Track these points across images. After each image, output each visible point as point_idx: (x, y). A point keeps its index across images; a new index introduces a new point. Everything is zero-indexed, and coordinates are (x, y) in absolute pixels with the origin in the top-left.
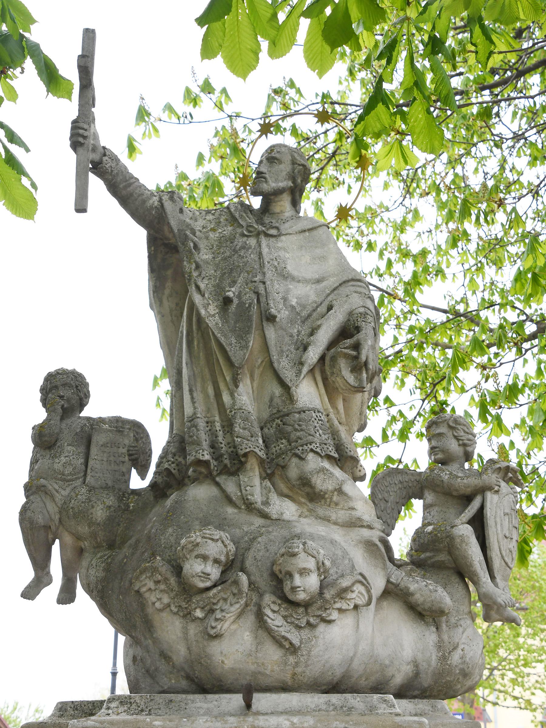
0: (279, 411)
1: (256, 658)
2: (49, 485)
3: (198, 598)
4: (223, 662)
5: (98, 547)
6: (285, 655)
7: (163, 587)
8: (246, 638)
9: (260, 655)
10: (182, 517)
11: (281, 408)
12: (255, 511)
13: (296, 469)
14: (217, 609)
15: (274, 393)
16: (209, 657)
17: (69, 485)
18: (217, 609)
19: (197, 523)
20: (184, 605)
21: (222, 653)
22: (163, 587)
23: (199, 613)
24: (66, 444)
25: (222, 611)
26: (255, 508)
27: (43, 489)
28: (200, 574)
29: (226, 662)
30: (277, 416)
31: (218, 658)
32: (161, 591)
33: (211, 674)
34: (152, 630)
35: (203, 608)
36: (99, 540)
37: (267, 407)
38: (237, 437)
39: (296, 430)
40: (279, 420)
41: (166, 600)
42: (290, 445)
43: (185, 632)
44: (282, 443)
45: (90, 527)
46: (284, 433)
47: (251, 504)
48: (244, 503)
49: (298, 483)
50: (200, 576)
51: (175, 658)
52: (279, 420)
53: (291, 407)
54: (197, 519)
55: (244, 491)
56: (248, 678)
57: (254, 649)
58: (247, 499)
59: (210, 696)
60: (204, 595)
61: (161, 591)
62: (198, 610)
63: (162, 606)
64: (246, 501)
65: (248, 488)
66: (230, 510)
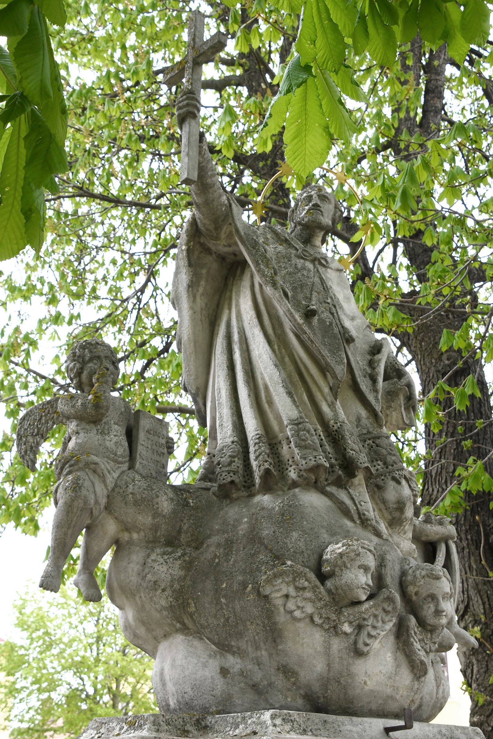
0: (369, 432)
1: (394, 681)
2: (101, 464)
3: (350, 610)
4: (365, 683)
5: (153, 542)
6: (413, 681)
7: (308, 594)
8: (388, 659)
9: (397, 678)
10: (305, 523)
11: (371, 430)
12: (370, 528)
13: (394, 492)
14: (368, 625)
15: (361, 414)
16: (351, 675)
17: (119, 467)
18: (368, 625)
19: (324, 531)
20: (333, 617)
21: (366, 673)
22: (308, 594)
23: (347, 628)
24: (112, 422)
25: (374, 627)
26: (371, 525)
27: (92, 466)
28: (364, 586)
29: (368, 683)
30: (368, 436)
31: (361, 678)
32: (305, 599)
33: (345, 694)
34: (278, 641)
35: (350, 623)
36: (159, 534)
37: (354, 426)
38: (352, 450)
39: (390, 454)
40: (371, 441)
41: (309, 609)
42: (387, 468)
43: (327, 647)
44: (379, 465)
45: (154, 517)
46: (379, 455)
47: (367, 520)
48: (360, 518)
49: (395, 506)
50: (364, 588)
51: (302, 674)
52: (371, 441)
53: (379, 430)
54: (322, 527)
55: (359, 506)
56: (380, 701)
57: (393, 672)
58: (364, 515)
59: (355, 719)
60: (356, 609)
61: (305, 599)
62: (346, 624)
63: (303, 615)
64: (362, 517)
65: (363, 503)
66: (349, 524)
